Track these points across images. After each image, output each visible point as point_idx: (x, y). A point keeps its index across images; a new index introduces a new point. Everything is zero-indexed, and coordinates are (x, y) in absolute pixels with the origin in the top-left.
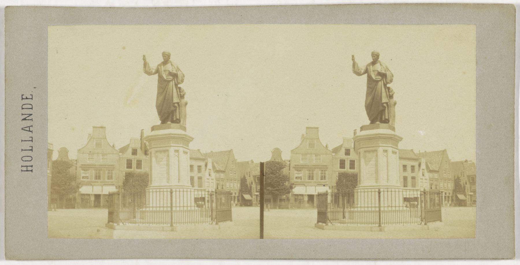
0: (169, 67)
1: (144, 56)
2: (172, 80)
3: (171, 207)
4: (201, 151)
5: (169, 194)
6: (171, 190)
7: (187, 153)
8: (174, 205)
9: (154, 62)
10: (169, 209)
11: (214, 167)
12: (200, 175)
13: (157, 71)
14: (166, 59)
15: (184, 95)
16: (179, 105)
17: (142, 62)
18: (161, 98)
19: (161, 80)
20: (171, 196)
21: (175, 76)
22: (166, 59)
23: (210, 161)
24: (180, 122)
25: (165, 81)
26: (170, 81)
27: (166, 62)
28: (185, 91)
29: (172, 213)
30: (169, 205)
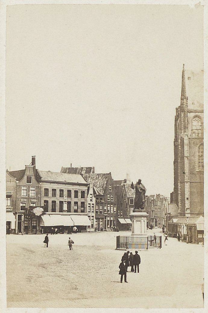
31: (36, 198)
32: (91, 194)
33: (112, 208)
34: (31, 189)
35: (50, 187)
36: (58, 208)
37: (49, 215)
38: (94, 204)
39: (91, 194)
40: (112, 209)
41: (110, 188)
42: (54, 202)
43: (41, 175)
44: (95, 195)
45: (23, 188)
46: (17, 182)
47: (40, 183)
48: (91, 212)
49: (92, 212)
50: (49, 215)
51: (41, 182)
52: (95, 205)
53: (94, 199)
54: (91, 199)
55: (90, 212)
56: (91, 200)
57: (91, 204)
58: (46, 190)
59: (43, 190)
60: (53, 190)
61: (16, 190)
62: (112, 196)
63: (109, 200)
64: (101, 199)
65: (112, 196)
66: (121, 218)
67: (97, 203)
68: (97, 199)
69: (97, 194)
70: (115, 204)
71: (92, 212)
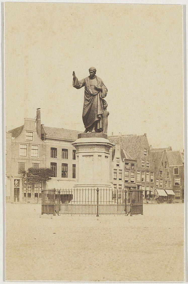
0: (94, 82)
1: (74, 72)
3: (98, 202)
6: (98, 189)
9: (83, 75)
10: (96, 203)
13: (84, 84)
14: (93, 74)
17: (72, 77)
18: (87, 110)
19: (87, 93)
20: (98, 194)
21: (100, 90)
22: (93, 74)
24: (103, 130)
25: (91, 95)
26: (96, 95)
29: (98, 206)
31: (39, 160)
32: (117, 158)
33: (147, 176)
34: (33, 147)
35: (60, 146)
36: (70, 173)
37: (58, 180)
38: (121, 170)
39: (117, 158)
40: (147, 178)
41: (145, 153)
42: (65, 165)
43: (46, 131)
44: (124, 159)
45: (21, 146)
46: (13, 138)
47: (45, 141)
48: (118, 179)
49: (120, 179)
50: (58, 180)
51: (46, 139)
52: (123, 171)
53: (122, 165)
54: (118, 164)
55: (116, 179)
56: (118, 165)
57: (118, 170)
58: (54, 150)
59: (49, 150)
60: (63, 150)
61: (11, 149)
62: (147, 162)
63: (143, 166)
64: (133, 165)
65: (147, 162)
66: (161, 189)
67: (126, 169)
68: (127, 164)
69: (127, 158)
70: (152, 173)
71: (114, 179)
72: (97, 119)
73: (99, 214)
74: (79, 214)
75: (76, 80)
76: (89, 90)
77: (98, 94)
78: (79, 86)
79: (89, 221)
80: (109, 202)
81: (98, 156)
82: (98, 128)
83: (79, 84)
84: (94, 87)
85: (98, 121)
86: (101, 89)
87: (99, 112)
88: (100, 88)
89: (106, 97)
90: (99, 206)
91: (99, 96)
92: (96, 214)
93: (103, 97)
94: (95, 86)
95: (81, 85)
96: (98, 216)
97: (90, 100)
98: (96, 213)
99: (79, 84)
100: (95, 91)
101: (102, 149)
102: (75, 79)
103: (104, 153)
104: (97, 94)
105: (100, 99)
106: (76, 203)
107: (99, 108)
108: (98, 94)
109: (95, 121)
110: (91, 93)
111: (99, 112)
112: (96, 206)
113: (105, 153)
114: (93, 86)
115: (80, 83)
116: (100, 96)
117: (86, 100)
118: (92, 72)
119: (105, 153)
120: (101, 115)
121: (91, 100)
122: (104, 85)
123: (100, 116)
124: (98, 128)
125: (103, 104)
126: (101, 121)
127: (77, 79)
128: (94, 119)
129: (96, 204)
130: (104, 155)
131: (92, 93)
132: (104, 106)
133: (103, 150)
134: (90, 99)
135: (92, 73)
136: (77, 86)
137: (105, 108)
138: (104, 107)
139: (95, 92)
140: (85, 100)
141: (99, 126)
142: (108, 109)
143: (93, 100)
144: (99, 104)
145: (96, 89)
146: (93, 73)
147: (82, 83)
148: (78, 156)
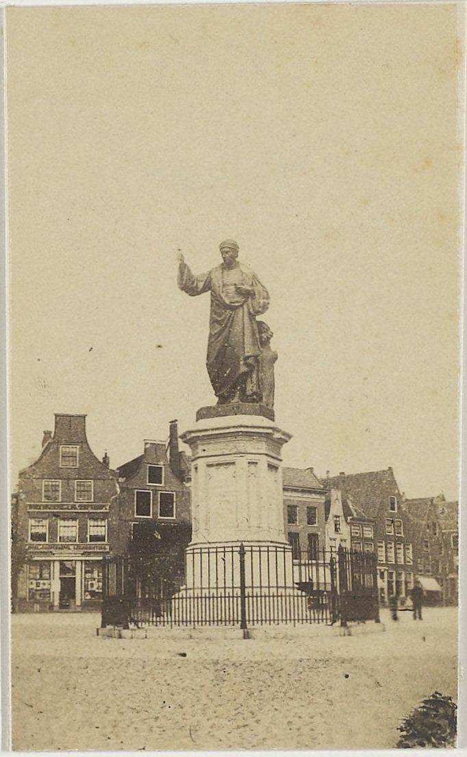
0: (233, 277)
2: (242, 306)
3: (243, 587)
4: (315, 472)
5: (237, 556)
6: (242, 547)
7: (277, 468)
8: (248, 583)
10: (238, 591)
11: (347, 512)
12: (311, 529)
15: (268, 339)
16: (257, 361)
21: (249, 295)
23: (336, 495)
25: (227, 307)
26: (237, 307)
27: (229, 263)
28: (272, 329)
30: (238, 583)
72: (243, 369)
73: (247, 622)
74: (192, 623)
75: (186, 272)
76: (220, 295)
77: (243, 304)
78: (197, 287)
79: (225, 643)
80: (277, 587)
81: (249, 463)
82: (249, 392)
83: (195, 283)
84: (233, 288)
85: (247, 375)
86: (251, 290)
87: (249, 350)
88: (250, 288)
89: (267, 313)
90: (247, 599)
91: (246, 309)
92: (240, 622)
93: (258, 313)
94: (237, 283)
95: (201, 285)
96: (243, 626)
97: (223, 320)
98: (240, 619)
99: (194, 282)
100: (240, 299)
101: (259, 445)
102: (183, 268)
103: (265, 457)
104: (242, 306)
105: (252, 316)
106: (190, 593)
107: (248, 339)
108: (245, 306)
109: (237, 375)
110: (225, 303)
111: (249, 350)
112: (239, 599)
113: (266, 455)
114: (231, 285)
115: (198, 281)
116: (249, 310)
117: (213, 322)
118: (228, 249)
119: (266, 455)
120: (256, 357)
121: (226, 321)
122: (259, 282)
123: (250, 361)
124: (249, 392)
125: (260, 332)
126: (254, 376)
127: (189, 271)
128: (238, 368)
129: (239, 594)
130: (263, 461)
131: (228, 303)
132: (261, 338)
133: (263, 447)
134: (222, 318)
135: (227, 252)
136: (190, 287)
137: (264, 343)
138: (263, 340)
139: (237, 299)
140: (212, 320)
141: (251, 387)
142: (273, 344)
143: (232, 324)
144: (248, 332)
145: (239, 291)
146: (230, 254)
147: (202, 281)
148: (196, 468)
